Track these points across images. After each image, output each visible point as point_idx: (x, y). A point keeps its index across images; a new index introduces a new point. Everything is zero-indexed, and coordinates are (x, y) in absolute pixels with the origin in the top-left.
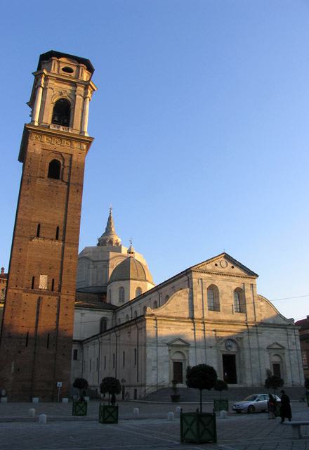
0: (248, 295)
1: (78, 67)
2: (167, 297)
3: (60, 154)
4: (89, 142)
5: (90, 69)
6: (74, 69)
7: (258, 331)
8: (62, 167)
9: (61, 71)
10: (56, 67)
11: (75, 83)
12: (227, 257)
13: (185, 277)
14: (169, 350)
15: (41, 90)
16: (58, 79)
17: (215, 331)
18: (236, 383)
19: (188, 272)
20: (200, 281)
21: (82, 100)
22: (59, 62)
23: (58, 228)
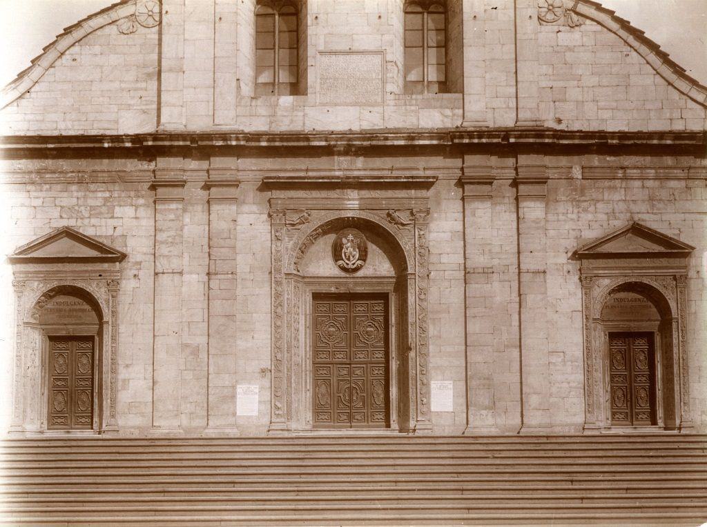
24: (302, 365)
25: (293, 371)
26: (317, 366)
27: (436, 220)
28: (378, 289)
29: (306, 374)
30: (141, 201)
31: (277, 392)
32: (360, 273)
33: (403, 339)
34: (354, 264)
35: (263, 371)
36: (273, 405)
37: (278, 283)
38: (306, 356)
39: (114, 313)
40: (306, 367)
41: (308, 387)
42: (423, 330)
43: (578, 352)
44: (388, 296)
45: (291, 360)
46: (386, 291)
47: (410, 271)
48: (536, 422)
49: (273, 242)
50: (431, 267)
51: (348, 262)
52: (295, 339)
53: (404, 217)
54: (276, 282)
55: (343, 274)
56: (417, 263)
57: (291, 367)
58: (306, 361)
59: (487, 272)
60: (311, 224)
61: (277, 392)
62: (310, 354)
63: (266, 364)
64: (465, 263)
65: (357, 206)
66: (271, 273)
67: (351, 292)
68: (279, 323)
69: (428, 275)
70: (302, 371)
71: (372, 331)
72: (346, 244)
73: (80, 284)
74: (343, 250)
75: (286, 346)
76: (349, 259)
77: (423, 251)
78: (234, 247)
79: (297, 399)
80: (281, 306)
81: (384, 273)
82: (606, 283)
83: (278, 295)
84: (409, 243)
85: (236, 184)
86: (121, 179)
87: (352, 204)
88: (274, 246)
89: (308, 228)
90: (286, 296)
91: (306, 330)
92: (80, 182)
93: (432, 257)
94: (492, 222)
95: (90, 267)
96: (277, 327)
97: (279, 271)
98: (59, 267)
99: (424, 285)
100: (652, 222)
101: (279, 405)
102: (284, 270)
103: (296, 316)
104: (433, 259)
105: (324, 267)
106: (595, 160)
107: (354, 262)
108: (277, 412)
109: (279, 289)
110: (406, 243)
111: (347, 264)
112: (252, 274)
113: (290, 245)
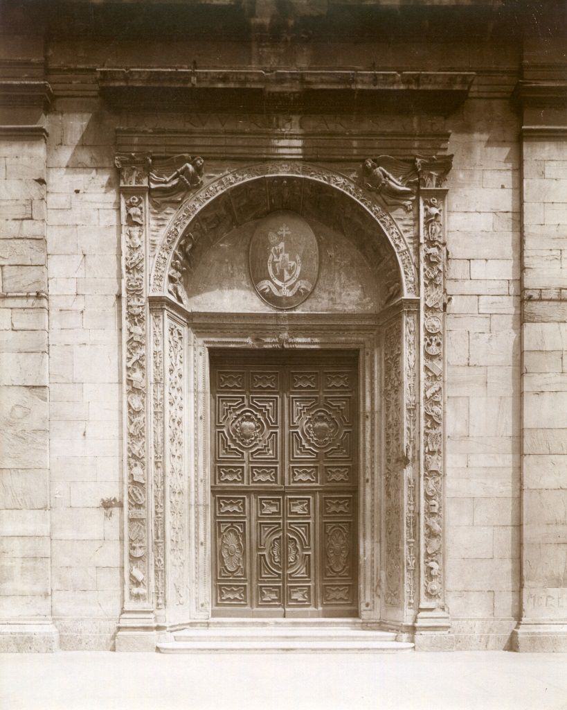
24: (189, 495)
25: (168, 504)
26: (219, 494)
27: (462, 186)
28: (341, 341)
29: (197, 512)
31: (134, 548)
33: (388, 443)
34: (291, 288)
35: (107, 505)
36: (127, 576)
37: (135, 319)
38: (196, 476)
40: (196, 497)
41: (202, 539)
42: (434, 422)
44: (358, 357)
45: (163, 483)
46: (353, 346)
47: (407, 295)
49: (124, 229)
50: (451, 288)
51: (279, 283)
52: (172, 440)
54: (131, 316)
56: (422, 280)
57: (164, 497)
58: (196, 486)
60: (201, 195)
61: (134, 548)
62: (206, 473)
63: (112, 491)
64: (521, 280)
65: (300, 151)
66: (119, 297)
67: (286, 346)
68: (136, 404)
69: (445, 306)
70: (190, 505)
71: (325, 429)
72: (277, 244)
74: (271, 258)
75: (153, 454)
76: (281, 278)
77: (433, 250)
78: (41, 240)
79: (177, 563)
80: (142, 367)
81: (351, 308)
83: (135, 344)
84: (406, 236)
88: (124, 238)
89: (198, 203)
90: (151, 347)
91: (196, 424)
93: (452, 264)
96: (134, 413)
97: (135, 292)
99: (435, 322)
101: (140, 577)
102: (149, 291)
103: (174, 392)
104: (457, 269)
108: (135, 590)
109: (137, 330)
111: (279, 288)
112: (81, 299)
113: (161, 237)
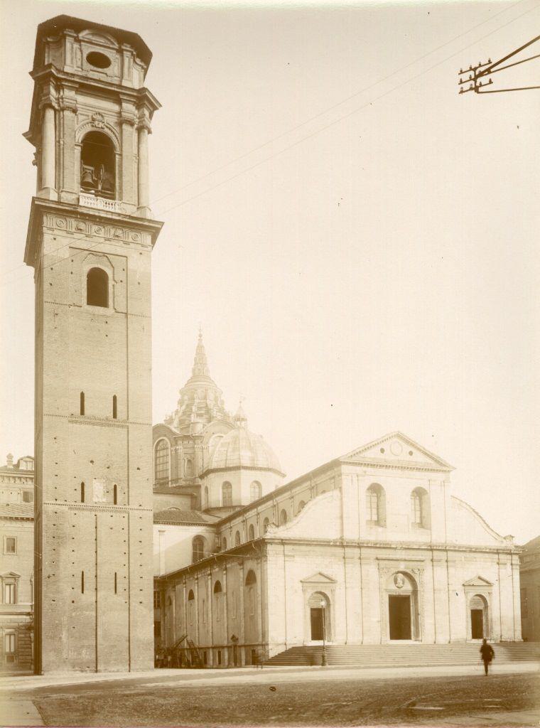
0: (435, 499)
1: (120, 51)
2: (303, 504)
3: (104, 255)
4: (153, 230)
5: (143, 54)
6: (111, 55)
7: (501, 561)
8: (111, 283)
9: (88, 66)
10: (73, 60)
11: (117, 94)
12: (399, 436)
13: (324, 477)
14: (304, 591)
15: (50, 114)
16: (82, 85)
17: (377, 559)
18: (408, 637)
19: (335, 464)
20: (355, 479)
21: (135, 135)
22: (77, 40)
23: (115, 398)
30: (339, 563)
32: (402, 589)
39: (334, 601)
43: (465, 617)
48: (454, 638)
53: (416, 571)
55: (397, 588)
59: (440, 590)
73: (323, 591)
82: (471, 595)
85: (369, 559)
86: (334, 555)
87: (402, 567)
92: (321, 555)
94: (440, 571)
95: (326, 585)
98: (316, 585)
100: (483, 576)
105: (393, 587)
106: (468, 555)
107: (401, 585)
110: (417, 580)
